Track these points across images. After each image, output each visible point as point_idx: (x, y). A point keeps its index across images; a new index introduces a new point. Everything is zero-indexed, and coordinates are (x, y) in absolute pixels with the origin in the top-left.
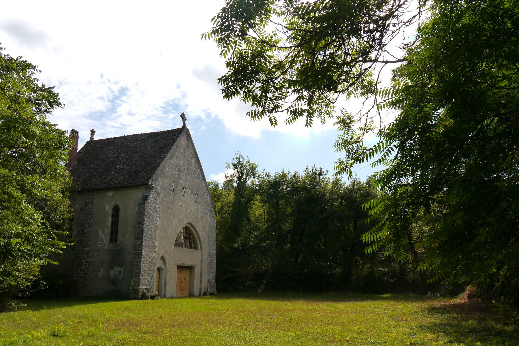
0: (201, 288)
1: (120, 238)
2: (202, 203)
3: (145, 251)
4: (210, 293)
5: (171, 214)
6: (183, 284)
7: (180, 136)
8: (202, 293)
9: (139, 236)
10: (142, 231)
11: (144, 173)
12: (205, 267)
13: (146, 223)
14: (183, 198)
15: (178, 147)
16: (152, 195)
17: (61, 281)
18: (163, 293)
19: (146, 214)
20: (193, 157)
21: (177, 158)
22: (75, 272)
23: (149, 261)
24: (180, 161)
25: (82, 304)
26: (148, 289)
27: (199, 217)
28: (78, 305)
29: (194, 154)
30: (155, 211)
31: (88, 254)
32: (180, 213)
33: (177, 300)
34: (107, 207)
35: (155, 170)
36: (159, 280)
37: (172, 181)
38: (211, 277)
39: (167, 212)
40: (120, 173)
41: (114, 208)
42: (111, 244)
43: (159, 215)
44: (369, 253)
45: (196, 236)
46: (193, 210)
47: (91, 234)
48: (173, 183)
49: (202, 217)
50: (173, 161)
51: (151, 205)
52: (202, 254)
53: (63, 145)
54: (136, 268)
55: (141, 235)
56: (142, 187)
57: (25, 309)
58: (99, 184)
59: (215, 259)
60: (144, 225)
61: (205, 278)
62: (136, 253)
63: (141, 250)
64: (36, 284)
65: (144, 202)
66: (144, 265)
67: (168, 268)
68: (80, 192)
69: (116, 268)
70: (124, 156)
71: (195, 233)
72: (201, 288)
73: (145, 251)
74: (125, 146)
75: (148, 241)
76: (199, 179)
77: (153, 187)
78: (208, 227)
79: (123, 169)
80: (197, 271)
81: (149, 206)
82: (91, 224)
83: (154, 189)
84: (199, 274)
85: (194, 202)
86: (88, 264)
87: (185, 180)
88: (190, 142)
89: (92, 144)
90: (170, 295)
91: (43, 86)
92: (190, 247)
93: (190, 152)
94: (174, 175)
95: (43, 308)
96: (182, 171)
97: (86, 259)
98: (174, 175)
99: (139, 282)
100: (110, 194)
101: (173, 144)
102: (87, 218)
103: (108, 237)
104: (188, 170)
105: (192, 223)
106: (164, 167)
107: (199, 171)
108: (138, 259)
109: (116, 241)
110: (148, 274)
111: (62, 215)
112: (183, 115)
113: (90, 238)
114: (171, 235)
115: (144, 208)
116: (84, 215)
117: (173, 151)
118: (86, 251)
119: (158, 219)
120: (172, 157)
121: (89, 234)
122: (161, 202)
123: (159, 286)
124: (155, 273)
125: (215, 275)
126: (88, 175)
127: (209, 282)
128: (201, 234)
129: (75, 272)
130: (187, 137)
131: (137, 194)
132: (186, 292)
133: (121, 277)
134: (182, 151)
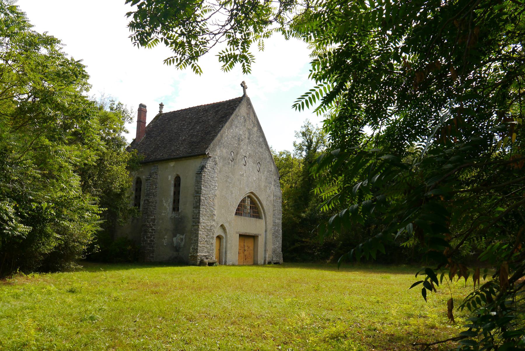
0: (265, 257)
1: (181, 207)
2: (266, 173)
3: (203, 219)
4: (275, 262)
5: (230, 183)
6: (246, 253)
7: (240, 104)
8: (267, 262)
9: (197, 205)
10: (200, 199)
11: (203, 143)
12: (270, 236)
13: (203, 192)
14: (244, 167)
15: (237, 116)
16: (209, 164)
17: (129, 248)
18: (224, 260)
19: (203, 183)
20: (254, 126)
21: (236, 127)
22: (142, 239)
23: (208, 229)
24: (240, 130)
25: (139, 268)
26: (207, 256)
27: (262, 186)
28: (135, 268)
29: (256, 123)
30: (213, 180)
31: (154, 222)
32: (241, 183)
33: (238, 268)
34: (170, 177)
35: (213, 139)
36: (220, 248)
37: (231, 151)
38: (277, 247)
39: (226, 181)
40: (182, 144)
41: (176, 178)
42: (174, 213)
43: (217, 185)
44: (325, 210)
45: (259, 205)
46: (255, 179)
47: (156, 203)
48: (232, 153)
49: (266, 187)
50: (232, 131)
51: (208, 174)
52: (266, 223)
53: (89, 115)
54: (194, 236)
55: (198, 204)
56: (200, 157)
57: (81, 270)
58: (162, 155)
59: (280, 228)
60: (201, 194)
61: (270, 247)
62: (194, 221)
63: (199, 219)
64: (91, 247)
65: (201, 171)
66: (202, 233)
67: (228, 236)
68: (145, 163)
69: (178, 235)
70: (187, 127)
71: (258, 202)
72: (265, 257)
73: (203, 219)
74: (189, 118)
75: (206, 209)
76: (262, 148)
77: (210, 157)
78: (272, 196)
79: (184, 140)
80: (261, 241)
81: (206, 175)
82: (156, 194)
83: (212, 158)
84: (264, 243)
85: (256, 171)
86: (154, 231)
87: (246, 149)
88: (251, 110)
89: (161, 118)
90: (231, 263)
91: (72, 60)
92: (254, 216)
93: (250, 120)
94: (233, 144)
95: (100, 270)
96: (242, 140)
97: (151, 227)
98: (233, 144)
99: (197, 249)
100: (172, 164)
101: (232, 114)
102: (151, 188)
103: (171, 206)
104: (249, 139)
105: (254, 192)
106: (222, 136)
107: (261, 140)
108: (196, 227)
109: (178, 210)
110: (206, 241)
111: (122, 184)
112: (243, 84)
113: (155, 207)
114: (231, 204)
115: (201, 177)
116: (149, 185)
117: (232, 120)
118: (151, 219)
119: (216, 188)
120: (231, 126)
121: (154, 203)
122: (220, 172)
123: (220, 253)
124: (215, 241)
125: (281, 245)
126: (154, 147)
127: (274, 251)
128: (264, 203)
129: (142, 239)
130: (248, 105)
131: (195, 164)
132: (251, 261)
133: (183, 244)
134: (242, 120)
